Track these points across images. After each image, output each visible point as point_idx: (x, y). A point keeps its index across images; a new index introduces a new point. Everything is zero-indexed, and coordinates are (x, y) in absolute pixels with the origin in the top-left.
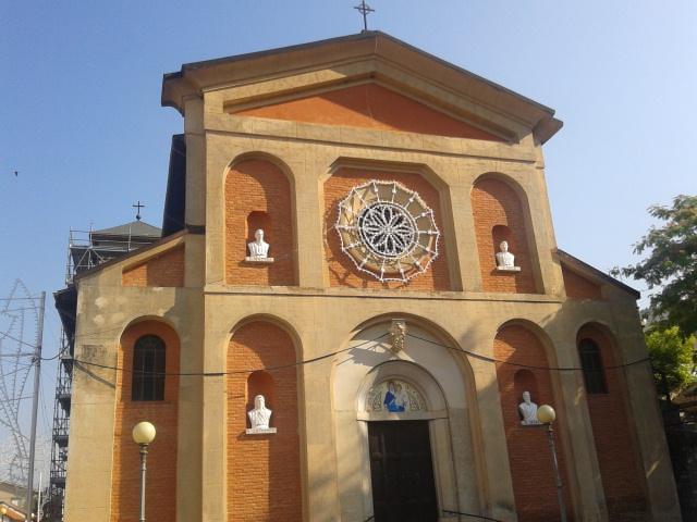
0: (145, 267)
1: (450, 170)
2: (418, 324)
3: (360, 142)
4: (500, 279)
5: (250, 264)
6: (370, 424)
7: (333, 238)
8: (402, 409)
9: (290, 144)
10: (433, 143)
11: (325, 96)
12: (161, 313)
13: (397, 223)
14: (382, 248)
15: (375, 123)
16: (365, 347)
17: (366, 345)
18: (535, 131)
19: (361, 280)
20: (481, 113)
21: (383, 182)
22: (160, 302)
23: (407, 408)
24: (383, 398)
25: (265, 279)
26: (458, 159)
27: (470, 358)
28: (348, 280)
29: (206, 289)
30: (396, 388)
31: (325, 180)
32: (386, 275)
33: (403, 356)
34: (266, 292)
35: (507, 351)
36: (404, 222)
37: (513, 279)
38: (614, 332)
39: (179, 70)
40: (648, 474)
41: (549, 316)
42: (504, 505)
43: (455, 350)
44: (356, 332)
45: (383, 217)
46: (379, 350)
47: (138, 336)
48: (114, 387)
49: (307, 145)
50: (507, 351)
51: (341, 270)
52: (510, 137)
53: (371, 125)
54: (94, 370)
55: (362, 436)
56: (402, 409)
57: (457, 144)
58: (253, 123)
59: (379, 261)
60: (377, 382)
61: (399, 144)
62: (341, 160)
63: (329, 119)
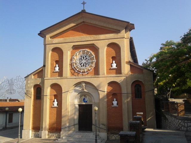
0: (37, 74)
1: (98, 44)
2: (86, 83)
3: (78, 41)
4: (111, 71)
5: (55, 72)
6: (79, 105)
7: (71, 65)
8: (87, 102)
9: (63, 44)
10: (96, 37)
11: (72, 30)
12: (38, 84)
13: (86, 60)
14: (82, 66)
15: (84, 34)
16: (77, 89)
17: (78, 88)
18: (126, 28)
19: (77, 74)
20: (110, 26)
21: (83, 50)
22: (38, 81)
23: (88, 102)
24: (83, 99)
25: (57, 75)
26: (102, 41)
27: (99, 91)
28: (74, 74)
29: (45, 79)
30: (86, 97)
31: (71, 51)
32: (82, 72)
33: (85, 91)
34: (56, 78)
35: (111, 88)
36: (87, 59)
37: (115, 70)
38: (143, 83)
39: (40, 32)
40: (147, 120)
41: (121, 80)
42: (103, 125)
43: (96, 89)
44: (75, 86)
45: (83, 58)
46: (80, 89)
47: (36, 88)
48: (31, 98)
49: (66, 43)
50: (111, 88)
51: (73, 72)
52: (118, 31)
53: (83, 35)
54: (28, 95)
55: (76, 108)
56: (87, 102)
57: (102, 36)
58: (56, 40)
59: (81, 69)
60: (81, 96)
61: (87, 39)
62: (74, 46)
63: (73, 36)
